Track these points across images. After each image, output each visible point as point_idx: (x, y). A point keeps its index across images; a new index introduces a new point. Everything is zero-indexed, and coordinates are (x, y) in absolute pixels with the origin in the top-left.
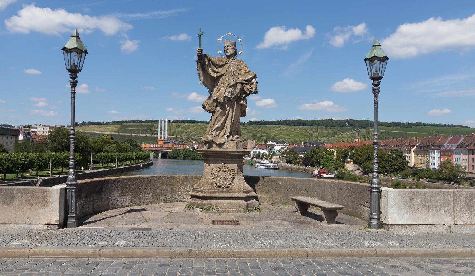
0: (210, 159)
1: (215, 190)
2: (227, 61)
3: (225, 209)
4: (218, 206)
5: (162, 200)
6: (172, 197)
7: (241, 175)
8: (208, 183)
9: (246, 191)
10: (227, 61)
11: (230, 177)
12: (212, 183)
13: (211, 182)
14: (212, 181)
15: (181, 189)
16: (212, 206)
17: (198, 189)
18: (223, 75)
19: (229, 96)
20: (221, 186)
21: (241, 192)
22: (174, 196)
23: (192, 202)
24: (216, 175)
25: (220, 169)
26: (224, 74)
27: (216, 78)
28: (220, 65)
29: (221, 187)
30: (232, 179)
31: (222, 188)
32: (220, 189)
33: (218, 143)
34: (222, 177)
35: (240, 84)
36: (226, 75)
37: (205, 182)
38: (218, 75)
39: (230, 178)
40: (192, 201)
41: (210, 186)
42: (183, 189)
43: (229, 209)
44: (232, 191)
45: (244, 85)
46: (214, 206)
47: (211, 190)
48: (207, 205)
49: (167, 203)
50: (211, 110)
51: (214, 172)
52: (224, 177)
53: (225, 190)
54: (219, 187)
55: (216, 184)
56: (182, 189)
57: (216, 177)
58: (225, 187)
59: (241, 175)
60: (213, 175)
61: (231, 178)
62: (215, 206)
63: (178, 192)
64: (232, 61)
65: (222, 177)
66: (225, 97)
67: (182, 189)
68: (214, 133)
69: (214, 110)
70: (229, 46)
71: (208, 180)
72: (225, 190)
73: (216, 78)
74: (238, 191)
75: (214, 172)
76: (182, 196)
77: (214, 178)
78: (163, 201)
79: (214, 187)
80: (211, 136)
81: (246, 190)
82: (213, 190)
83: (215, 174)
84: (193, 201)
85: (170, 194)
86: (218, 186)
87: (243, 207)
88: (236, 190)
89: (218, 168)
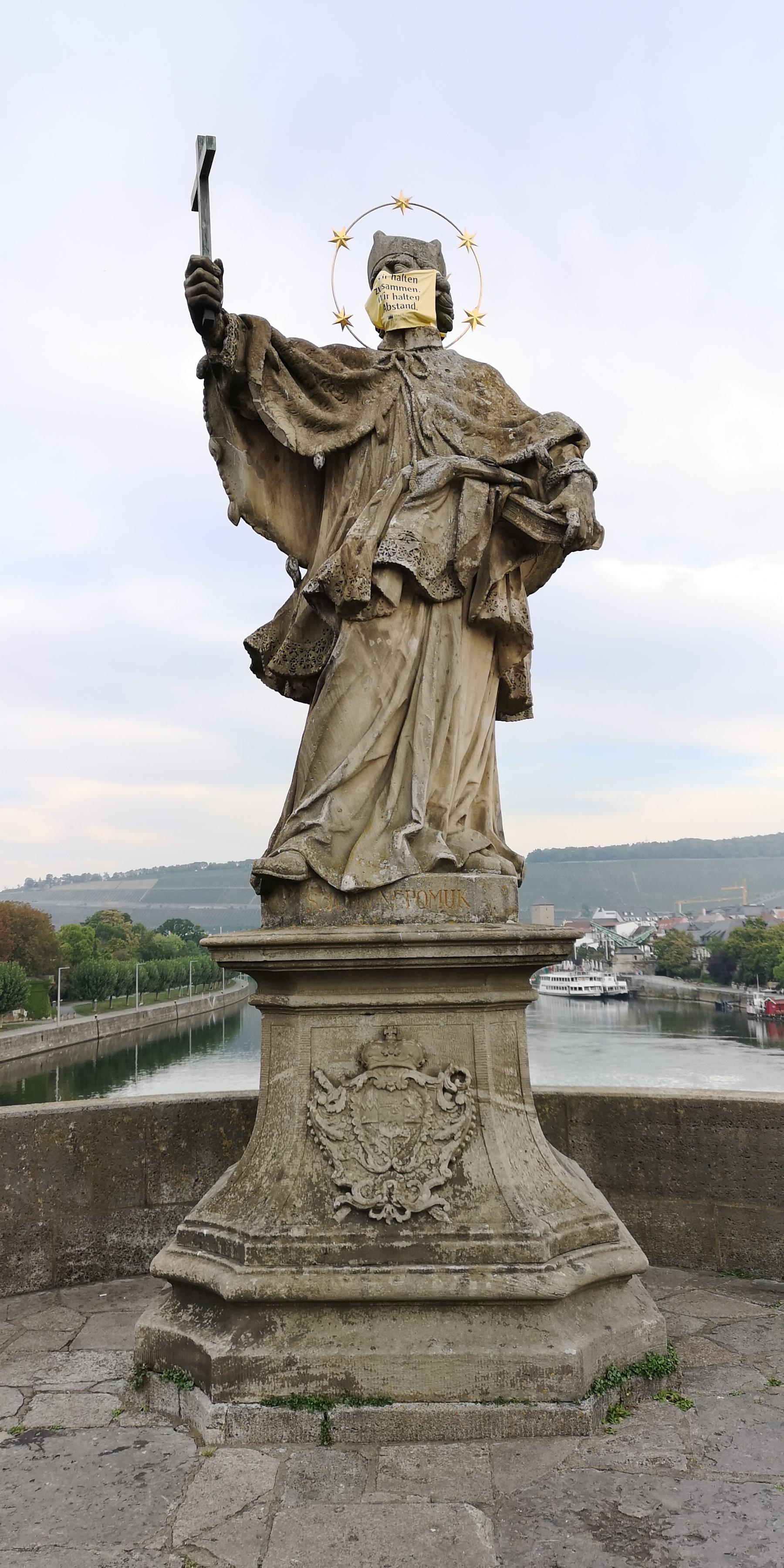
0: (295, 1000)
1: (329, 1240)
2: (389, 357)
3: (412, 1407)
4: (358, 1378)
5: (29, 1270)
6: (99, 1247)
7: (520, 1106)
8: (285, 1182)
9: (565, 1238)
10: (389, 357)
11: (441, 1135)
12: (314, 1180)
13: (308, 1169)
14: (313, 1167)
15: (157, 1189)
16: (313, 1378)
17: (216, 1233)
18: (366, 437)
19: (407, 565)
20: (377, 1210)
21: (527, 1253)
22: (114, 1236)
23: (169, 1334)
24: (336, 1119)
25: (363, 1077)
26: (374, 430)
27: (319, 461)
28: (341, 380)
29: (379, 1217)
30: (454, 1145)
31: (384, 1219)
32: (371, 1232)
33: (348, 883)
34: (384, 1131)
35: (477, 485)
36: (384, 441)
37: (267, 1172)
38: (331, 442)
39: (446, 1141)
40: (167, 1328)
41: (299, 1204)
42: (173, 1185)
43: (443, 1407)
44: (459, 1244)
45: (506, 491)
46: (322, 1377)
47: (302, 1239)
48: (273, 1371)
49: (71, 1285)
50: (300, 671)
51: (322, 1098)
52: (398, 1131)
53: (407, 1238)
54: (359, 1214)
55: (345, 1189)
56: (165, 1186)
57: (340, 1135)
58: (408, 1213)
59: (518, 1112)
60: (319, 1119)
61: (452, 1137)
62: (334, 1382)
63: (140, 1206)
64: (419, 354)
65: (384, 1131)
66: (379, 567)
67: (165, 1186)
68: (321, 820)
69: (314, 670)
70: (397, 267)
71: (287, 1157)
72: (407, 1238)
73: (319, 461)
74: (506, 1249)
75: (322, 1098)
76: (164, 1231)
77: (326, 1142)
78: (40, 1274)
79: (322, 1217)
80: (303, 839)
81: (568, 1231)
82: (321, 1239)
83: (330, 1108)
84: (175, 1330)
85: (89, 1226)
86: (353, 1209)
87: (552, 1381)
88: (488, 1237)
89: (351, 1066)
